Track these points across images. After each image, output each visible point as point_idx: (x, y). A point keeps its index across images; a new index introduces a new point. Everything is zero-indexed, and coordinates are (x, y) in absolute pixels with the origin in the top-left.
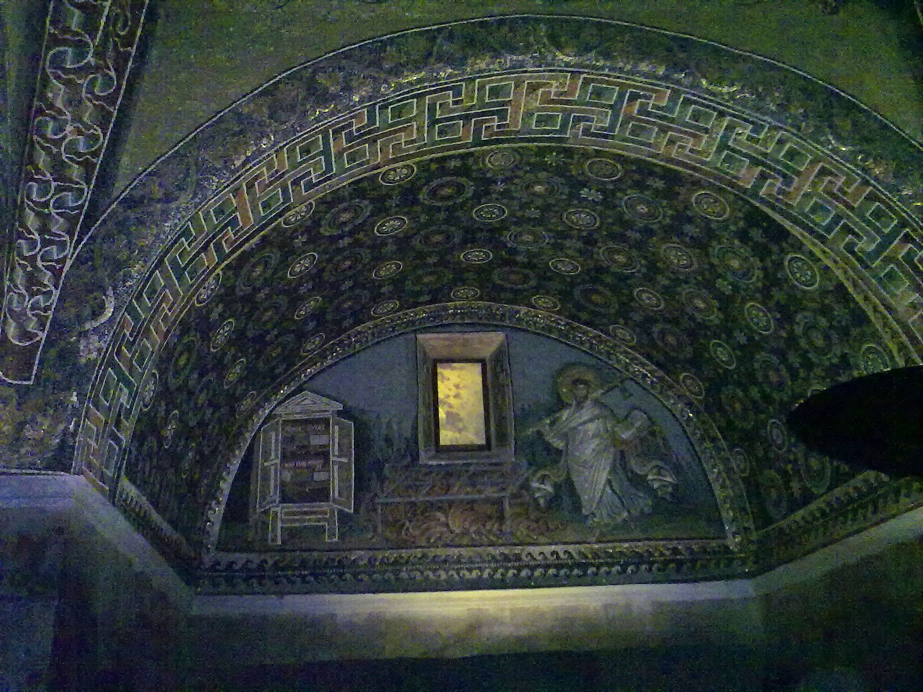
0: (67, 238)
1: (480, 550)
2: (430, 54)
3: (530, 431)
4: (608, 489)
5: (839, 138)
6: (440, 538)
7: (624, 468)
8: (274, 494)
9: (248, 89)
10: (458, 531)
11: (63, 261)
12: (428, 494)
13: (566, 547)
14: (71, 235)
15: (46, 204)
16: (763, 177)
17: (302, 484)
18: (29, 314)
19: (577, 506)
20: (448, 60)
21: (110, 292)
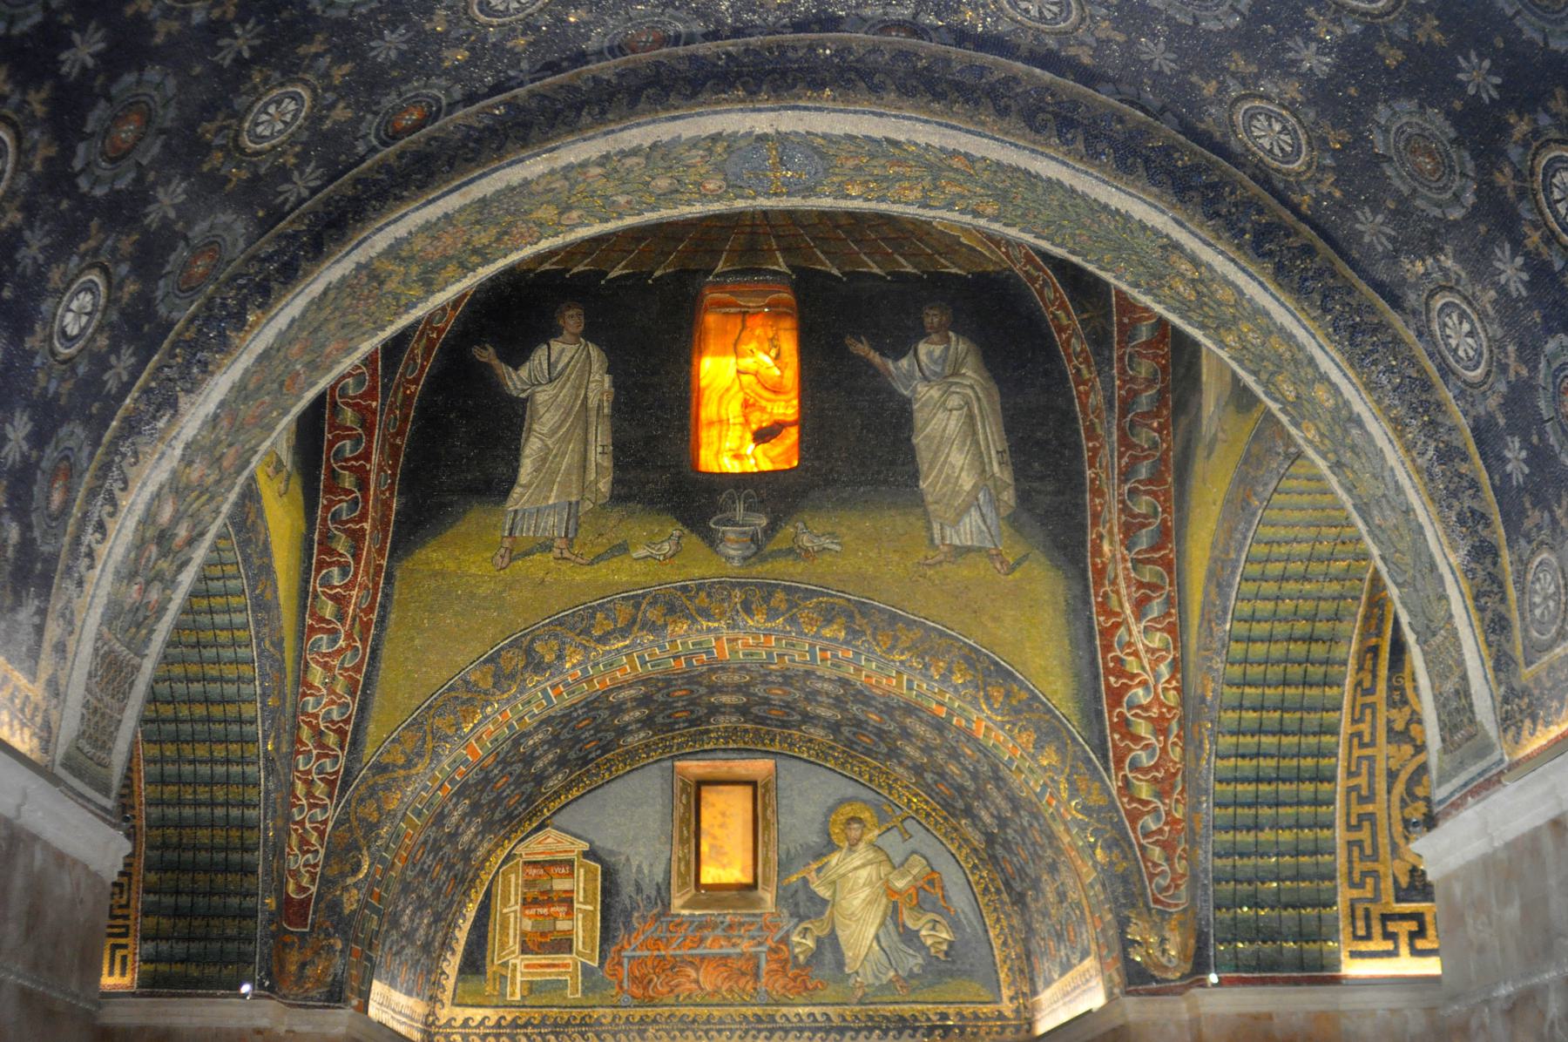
0: (327, 801)
1: (731, 1010)
2: (634, 622)
3: (794, 879)
4: (876, 947)
5: (991, 707)
6: (689, 996)
7: (896, 924)
8: (514, 944)
9: (475, 656)
10: (709, 988)
11: (325, 822)
12: (679, 947)
13: (824, 1009)
14: (330, 797)
15: (309, 772)
16: (950, 714)
17: (543, 934)
18: (303, 870)
19: (840, 964)
20: (652, 627)
21: (365, 852)
